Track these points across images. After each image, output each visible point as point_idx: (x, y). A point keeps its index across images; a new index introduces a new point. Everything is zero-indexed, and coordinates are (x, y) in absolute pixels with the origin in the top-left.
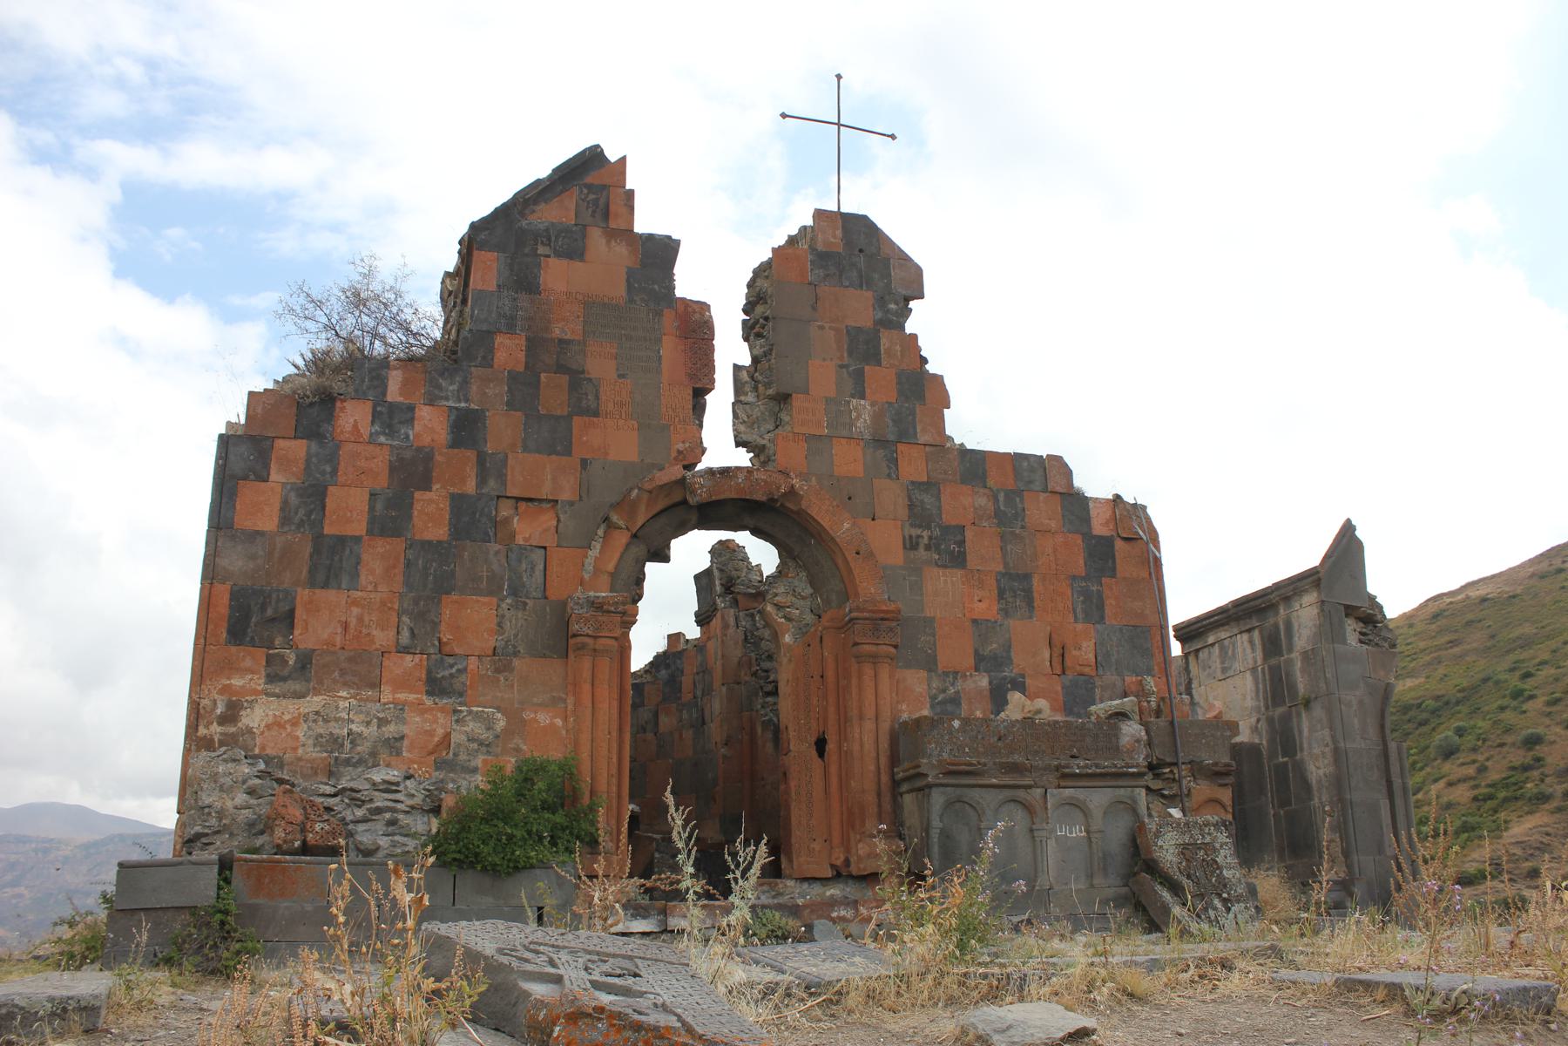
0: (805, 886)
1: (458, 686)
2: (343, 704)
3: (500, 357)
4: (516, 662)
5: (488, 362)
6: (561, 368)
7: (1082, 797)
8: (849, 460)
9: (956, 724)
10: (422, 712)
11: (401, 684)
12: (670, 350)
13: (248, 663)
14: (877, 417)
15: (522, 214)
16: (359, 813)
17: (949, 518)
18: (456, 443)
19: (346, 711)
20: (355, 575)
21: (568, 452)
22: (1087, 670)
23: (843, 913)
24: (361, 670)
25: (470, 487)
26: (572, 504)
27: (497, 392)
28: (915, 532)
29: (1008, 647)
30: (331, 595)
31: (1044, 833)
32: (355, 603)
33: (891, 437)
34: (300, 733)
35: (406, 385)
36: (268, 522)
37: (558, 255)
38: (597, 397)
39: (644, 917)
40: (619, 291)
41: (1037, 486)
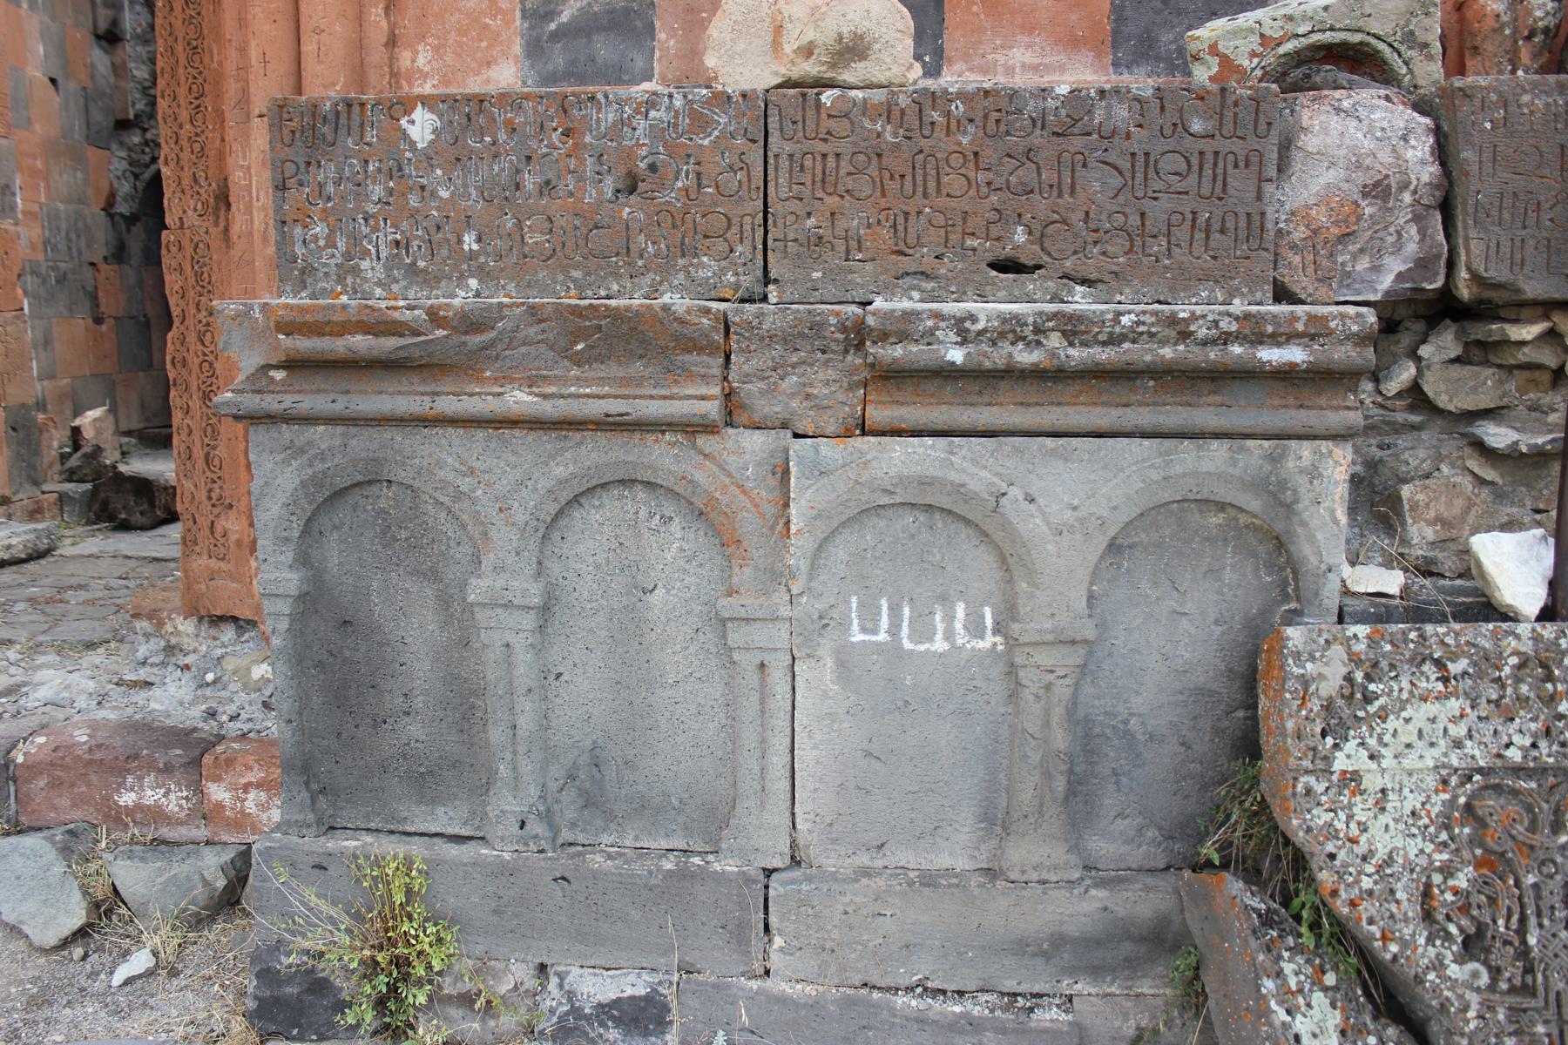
0: (228, 633)
23: (152, 796)
31: (780, 636)
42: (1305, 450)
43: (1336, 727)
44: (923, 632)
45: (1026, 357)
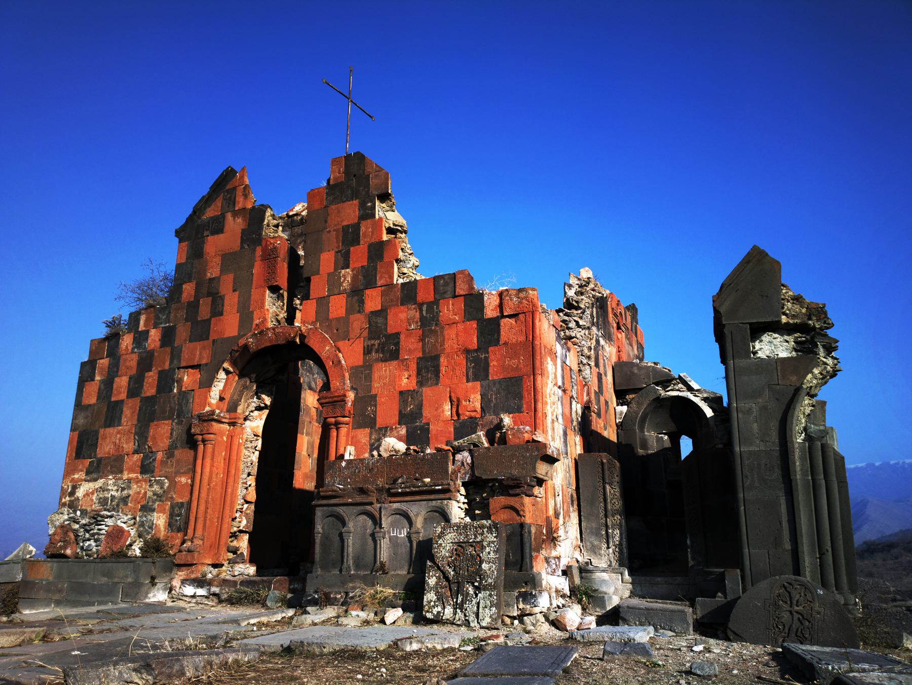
1: (152, 468)
2: (110, 482)
3: (184, 295)
4: (176, 452)
5: (179, 300)
6: (209, 294)
7: (404, 508)
8: (338, 306)
9: (344, 464)
10: (137, 483)
11: (131, 470)
12: (258, 269)
13: (80, 467)
14: (354, 278)
15: (199, 217)
16: (87, 535)
17: (390, 330)
18: (162, 346)
19: (111, 486)
20: (120, 419)
21: (207, 338)
22: (473, 414)
24: (115, 465)
25: (167, 366)
26: (206, 364)
27: (182, 313)
28: (370, 343)
29: (420, 406)
30: (111, 430)
32: (118, 432)
33: (362, 287)
34: (94, 498)
35: (146, 321)
36: (93, 401)
37: (213, 234)
38: (223, 305)
39: (202, 587)
40: (236, 245)
41: (449, 294)
42: (445, 502)
43: (440, 537)
44: (400, 534)
45: (408, 490)
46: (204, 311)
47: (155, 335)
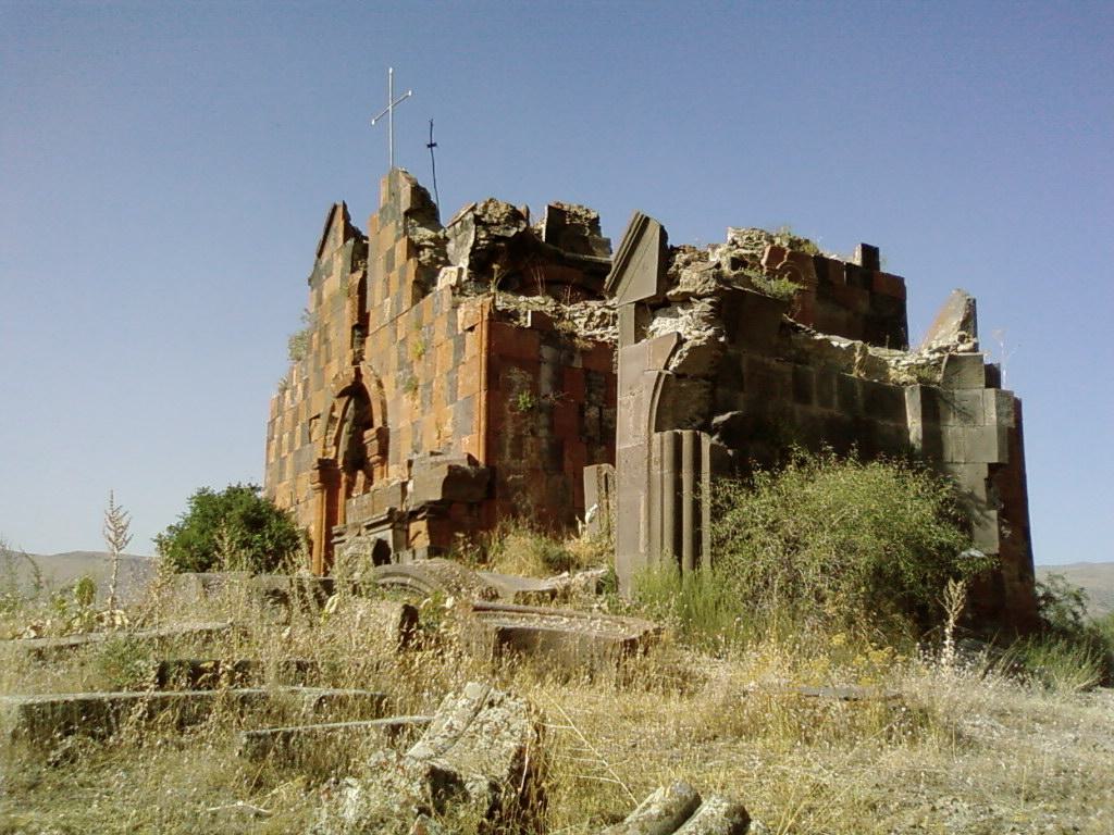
27: (311, 365)
46: (323, 356)
47: (300, 388)
